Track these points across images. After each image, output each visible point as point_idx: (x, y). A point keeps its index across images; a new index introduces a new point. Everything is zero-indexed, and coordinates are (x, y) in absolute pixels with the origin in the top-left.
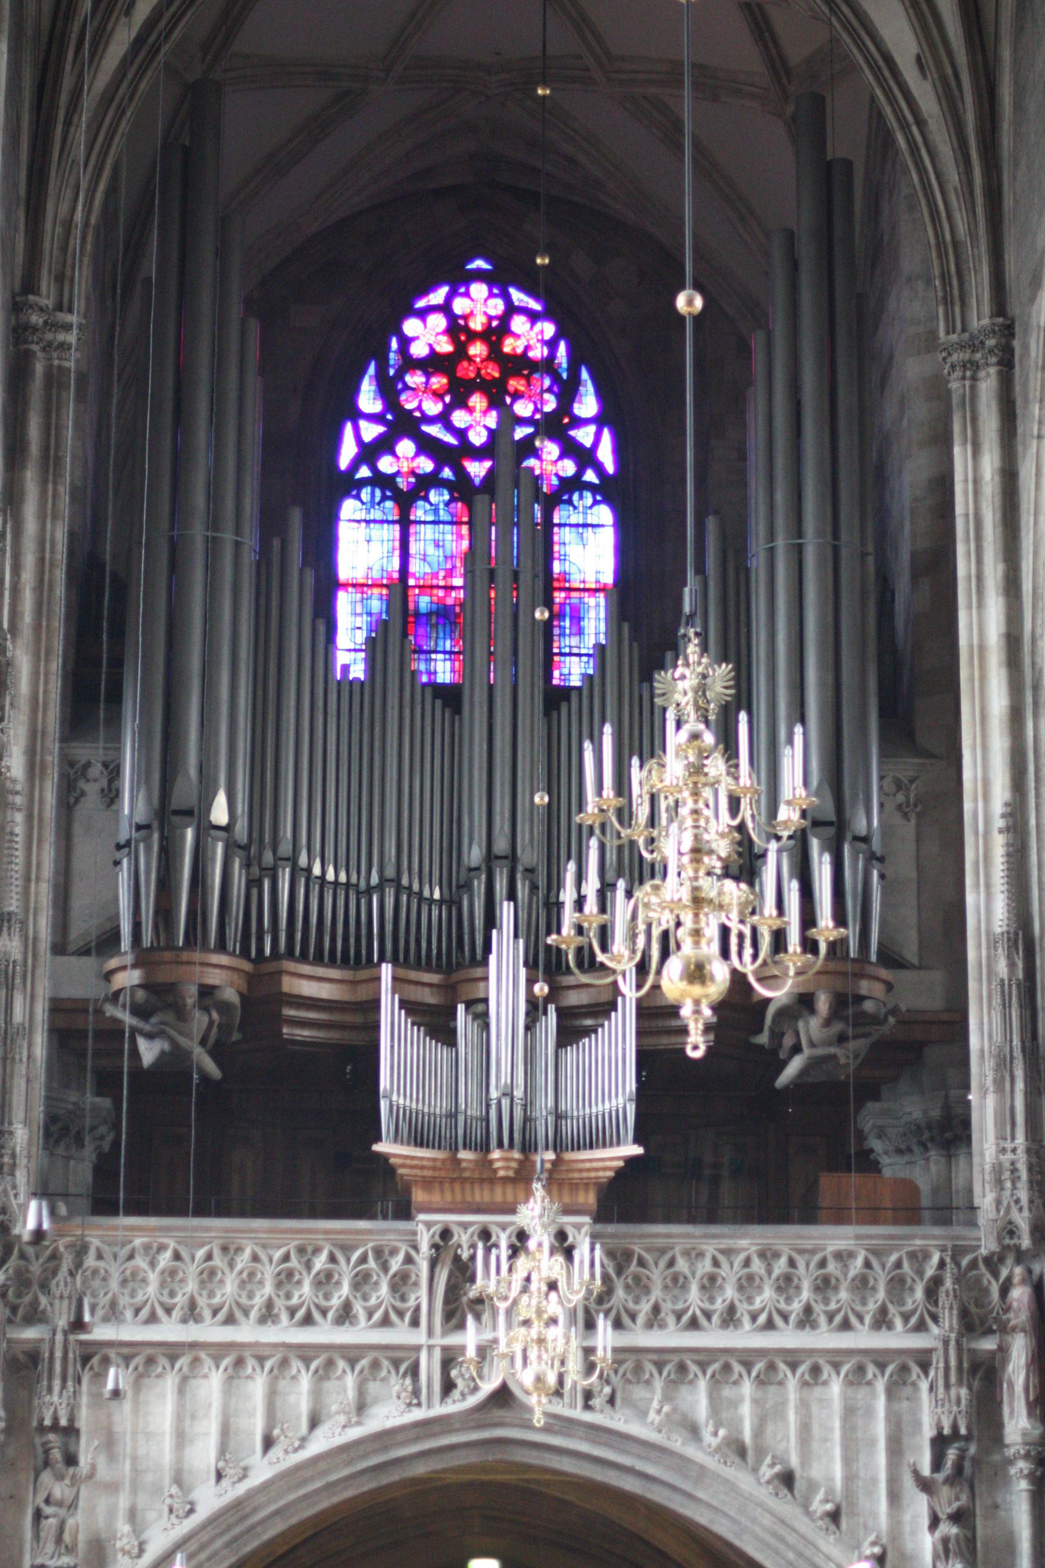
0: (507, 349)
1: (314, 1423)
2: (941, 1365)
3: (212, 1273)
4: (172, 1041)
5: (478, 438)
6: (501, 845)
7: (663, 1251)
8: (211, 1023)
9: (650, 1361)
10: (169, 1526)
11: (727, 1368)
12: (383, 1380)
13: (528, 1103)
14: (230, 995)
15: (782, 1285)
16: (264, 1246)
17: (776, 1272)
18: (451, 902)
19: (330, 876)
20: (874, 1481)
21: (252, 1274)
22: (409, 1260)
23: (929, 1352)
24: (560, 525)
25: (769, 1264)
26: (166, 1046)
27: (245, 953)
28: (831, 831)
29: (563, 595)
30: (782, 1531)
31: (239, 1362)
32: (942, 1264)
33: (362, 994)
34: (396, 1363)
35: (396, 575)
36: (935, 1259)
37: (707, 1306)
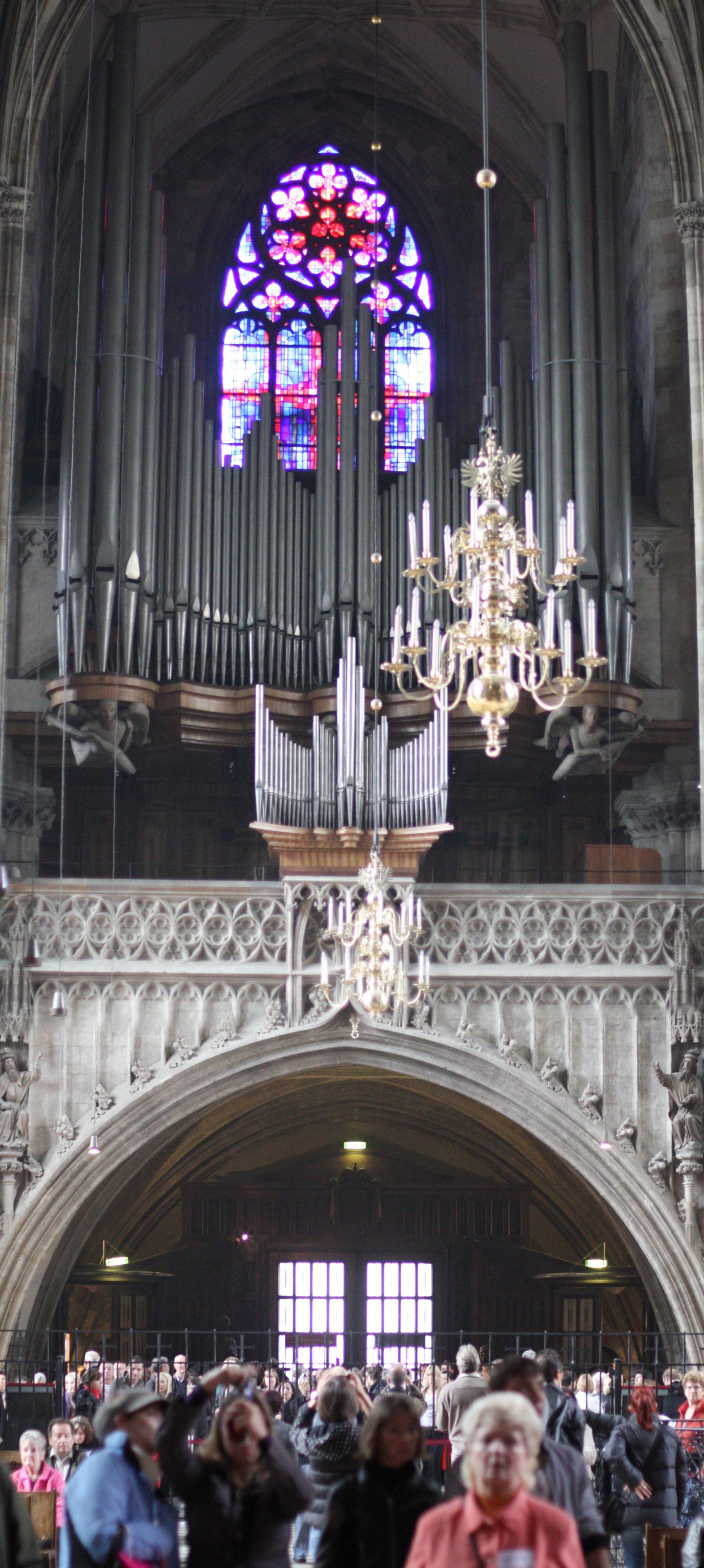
0: (350, 214)
2: (676, 989)
3: (130, 921)
4: (98, 744)
5: (328, 282)
6: (346, 594)
7: (468, 904)
8: (127, 730)
11: (515, 992)
12: (259, 1001)
13: (367, 792)
14: (142, 709)
15: (558, 929)
16: (169, 901)
17: (553, 919)
18: (308, 637)
19: (217, 617)
21: (160, 922)
23: (666, 979)
24: (390, 348)
25: (547, 914)
26: (94, 748)
27: (153, 677)
28: (595, 583)
29: (392, 401)
31: (151, 988)
32: (677, 914)
33: (241, 708)
34: (269, 989)
35: (266, 387)
36: (672, 910)
37: (500, 945)
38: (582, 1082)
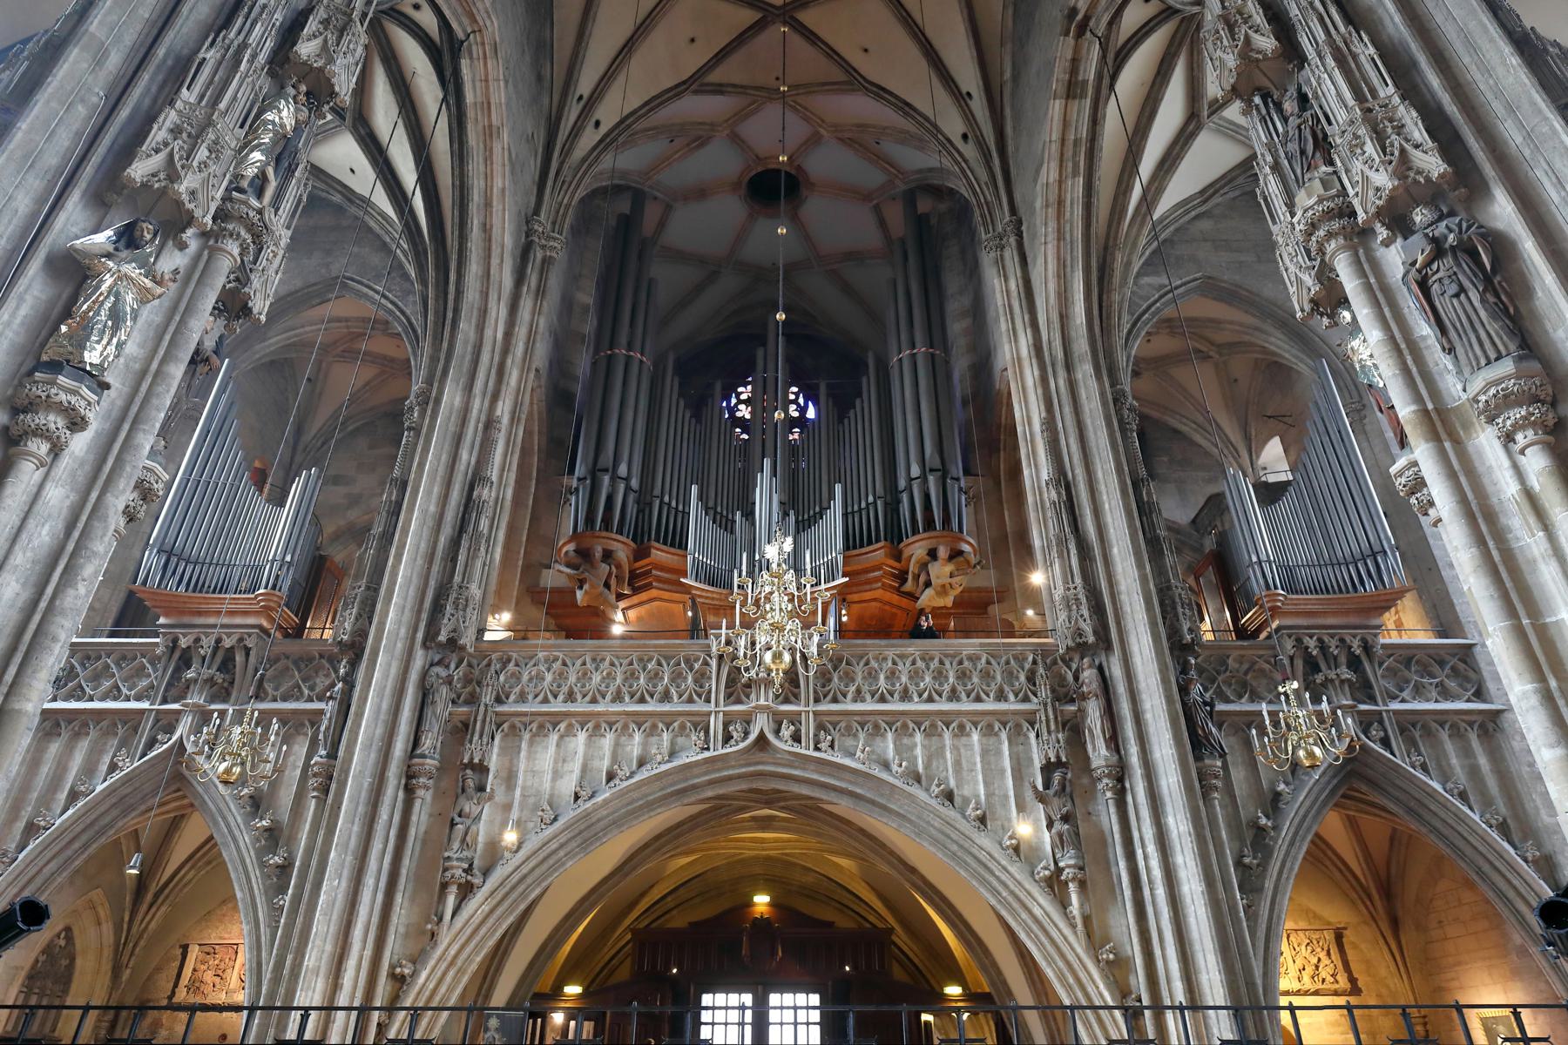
2: (1043, 718)
16: (618, 657)
20: (1006, 797)
22: (706, 663)
23: (1034, 712)
27: (634, 540)
28: (939, 473)
30: (948, 830)
32: (1035, 662)
34: (695, 725)
36: (1030, 659)
38: (966, 801)
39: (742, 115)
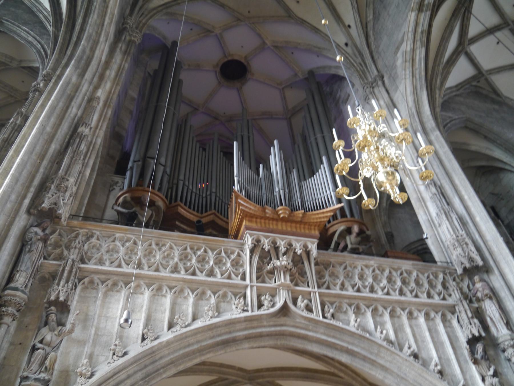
1: (194, 319)
3: (150, 253)
9: (346, 303)
10: (112, 361)
12: (228, 302)
39: (228, 28)
